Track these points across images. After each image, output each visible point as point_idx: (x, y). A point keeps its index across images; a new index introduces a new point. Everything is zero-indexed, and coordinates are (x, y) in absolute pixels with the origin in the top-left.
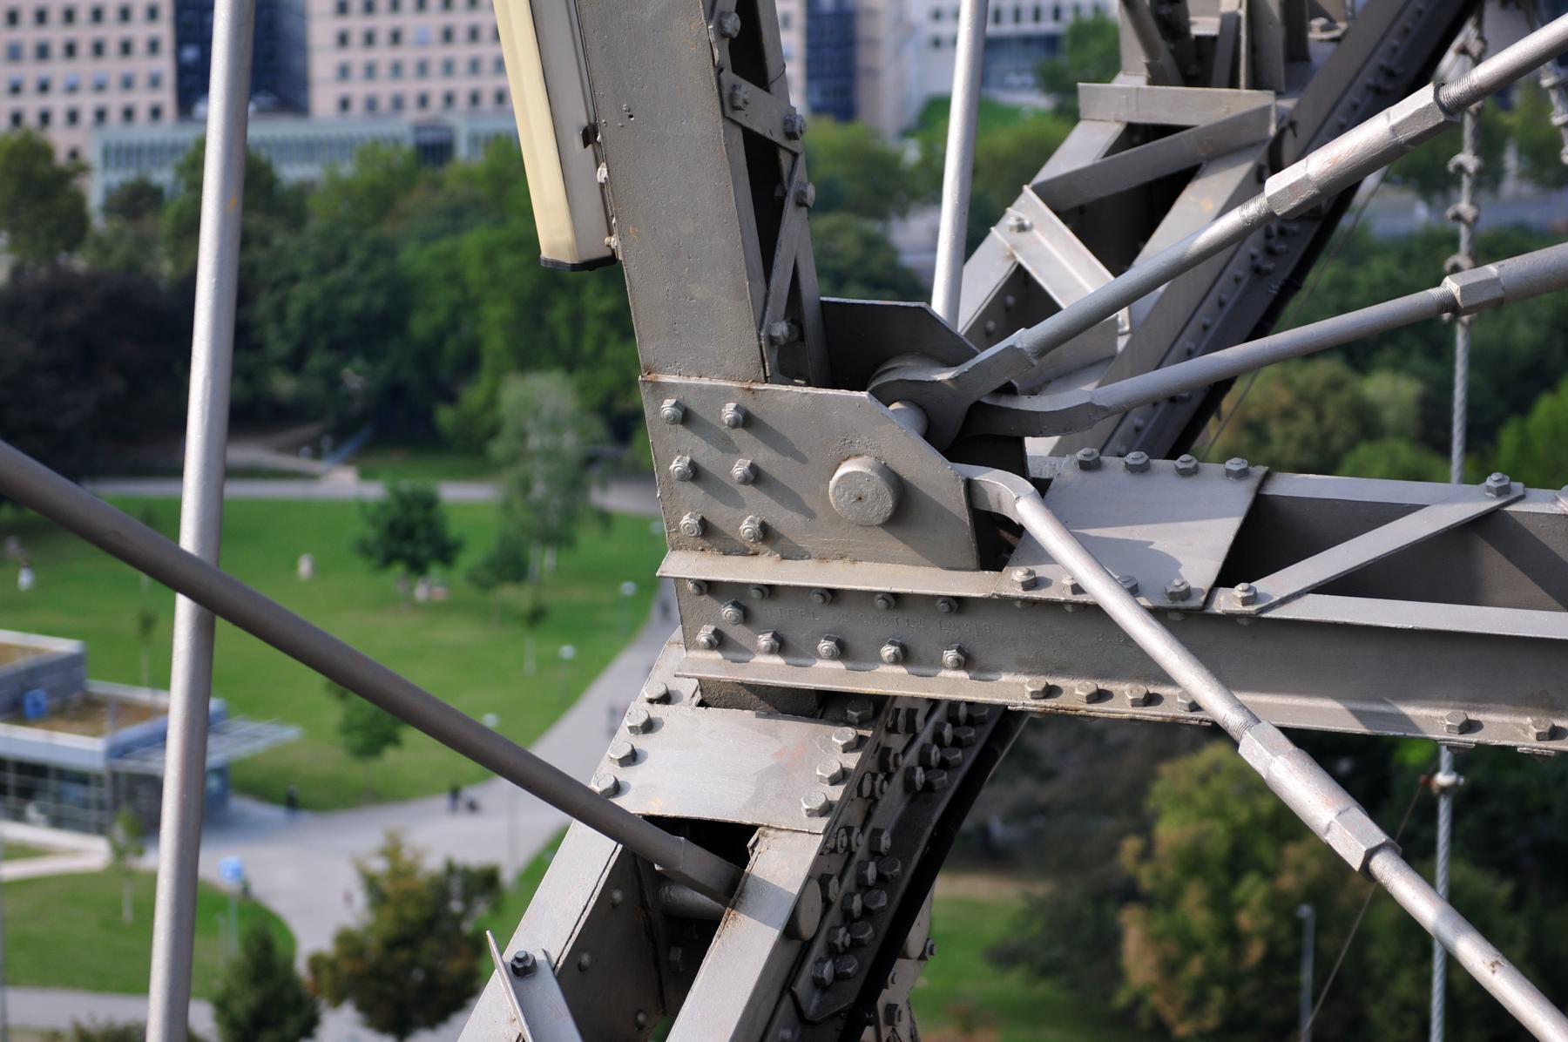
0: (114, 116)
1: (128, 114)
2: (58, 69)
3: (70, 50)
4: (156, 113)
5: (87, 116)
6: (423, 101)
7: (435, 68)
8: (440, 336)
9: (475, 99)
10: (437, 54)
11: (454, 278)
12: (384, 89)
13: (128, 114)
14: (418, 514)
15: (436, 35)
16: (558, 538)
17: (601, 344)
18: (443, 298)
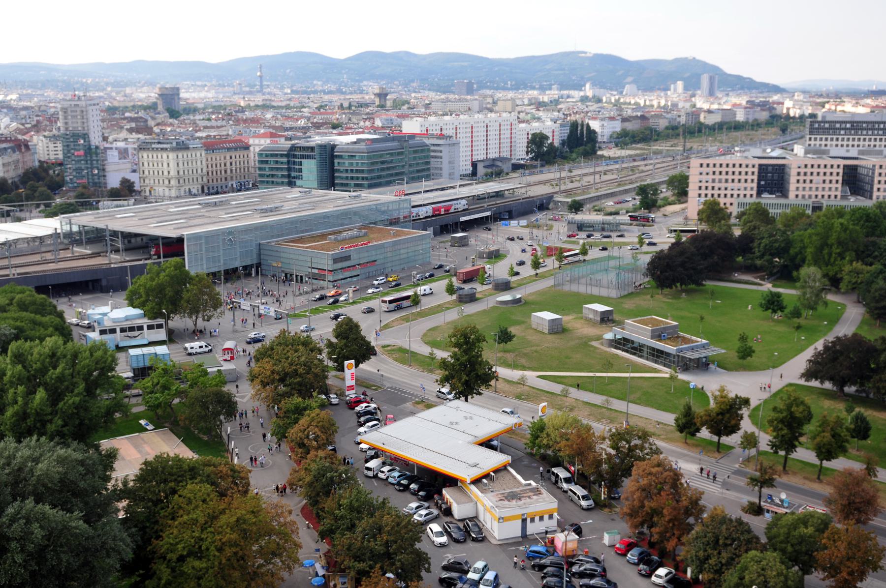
0: (742, 196)
1: (745, 196)
2: (730, 185)
3: (733, 181)
4: (751, 196)
5: (735, 196)
6: (816, 196)
7: (820, 189)
8: (797, 254)
9: (829, 196)
10: (821, 186)
11: (802, 241)
12: (807, 193)
13: (745, 196)
14: (776, 298)
15: (822, 181)
16: (813, 308)
17: (836, 260)
18: (798, 245)
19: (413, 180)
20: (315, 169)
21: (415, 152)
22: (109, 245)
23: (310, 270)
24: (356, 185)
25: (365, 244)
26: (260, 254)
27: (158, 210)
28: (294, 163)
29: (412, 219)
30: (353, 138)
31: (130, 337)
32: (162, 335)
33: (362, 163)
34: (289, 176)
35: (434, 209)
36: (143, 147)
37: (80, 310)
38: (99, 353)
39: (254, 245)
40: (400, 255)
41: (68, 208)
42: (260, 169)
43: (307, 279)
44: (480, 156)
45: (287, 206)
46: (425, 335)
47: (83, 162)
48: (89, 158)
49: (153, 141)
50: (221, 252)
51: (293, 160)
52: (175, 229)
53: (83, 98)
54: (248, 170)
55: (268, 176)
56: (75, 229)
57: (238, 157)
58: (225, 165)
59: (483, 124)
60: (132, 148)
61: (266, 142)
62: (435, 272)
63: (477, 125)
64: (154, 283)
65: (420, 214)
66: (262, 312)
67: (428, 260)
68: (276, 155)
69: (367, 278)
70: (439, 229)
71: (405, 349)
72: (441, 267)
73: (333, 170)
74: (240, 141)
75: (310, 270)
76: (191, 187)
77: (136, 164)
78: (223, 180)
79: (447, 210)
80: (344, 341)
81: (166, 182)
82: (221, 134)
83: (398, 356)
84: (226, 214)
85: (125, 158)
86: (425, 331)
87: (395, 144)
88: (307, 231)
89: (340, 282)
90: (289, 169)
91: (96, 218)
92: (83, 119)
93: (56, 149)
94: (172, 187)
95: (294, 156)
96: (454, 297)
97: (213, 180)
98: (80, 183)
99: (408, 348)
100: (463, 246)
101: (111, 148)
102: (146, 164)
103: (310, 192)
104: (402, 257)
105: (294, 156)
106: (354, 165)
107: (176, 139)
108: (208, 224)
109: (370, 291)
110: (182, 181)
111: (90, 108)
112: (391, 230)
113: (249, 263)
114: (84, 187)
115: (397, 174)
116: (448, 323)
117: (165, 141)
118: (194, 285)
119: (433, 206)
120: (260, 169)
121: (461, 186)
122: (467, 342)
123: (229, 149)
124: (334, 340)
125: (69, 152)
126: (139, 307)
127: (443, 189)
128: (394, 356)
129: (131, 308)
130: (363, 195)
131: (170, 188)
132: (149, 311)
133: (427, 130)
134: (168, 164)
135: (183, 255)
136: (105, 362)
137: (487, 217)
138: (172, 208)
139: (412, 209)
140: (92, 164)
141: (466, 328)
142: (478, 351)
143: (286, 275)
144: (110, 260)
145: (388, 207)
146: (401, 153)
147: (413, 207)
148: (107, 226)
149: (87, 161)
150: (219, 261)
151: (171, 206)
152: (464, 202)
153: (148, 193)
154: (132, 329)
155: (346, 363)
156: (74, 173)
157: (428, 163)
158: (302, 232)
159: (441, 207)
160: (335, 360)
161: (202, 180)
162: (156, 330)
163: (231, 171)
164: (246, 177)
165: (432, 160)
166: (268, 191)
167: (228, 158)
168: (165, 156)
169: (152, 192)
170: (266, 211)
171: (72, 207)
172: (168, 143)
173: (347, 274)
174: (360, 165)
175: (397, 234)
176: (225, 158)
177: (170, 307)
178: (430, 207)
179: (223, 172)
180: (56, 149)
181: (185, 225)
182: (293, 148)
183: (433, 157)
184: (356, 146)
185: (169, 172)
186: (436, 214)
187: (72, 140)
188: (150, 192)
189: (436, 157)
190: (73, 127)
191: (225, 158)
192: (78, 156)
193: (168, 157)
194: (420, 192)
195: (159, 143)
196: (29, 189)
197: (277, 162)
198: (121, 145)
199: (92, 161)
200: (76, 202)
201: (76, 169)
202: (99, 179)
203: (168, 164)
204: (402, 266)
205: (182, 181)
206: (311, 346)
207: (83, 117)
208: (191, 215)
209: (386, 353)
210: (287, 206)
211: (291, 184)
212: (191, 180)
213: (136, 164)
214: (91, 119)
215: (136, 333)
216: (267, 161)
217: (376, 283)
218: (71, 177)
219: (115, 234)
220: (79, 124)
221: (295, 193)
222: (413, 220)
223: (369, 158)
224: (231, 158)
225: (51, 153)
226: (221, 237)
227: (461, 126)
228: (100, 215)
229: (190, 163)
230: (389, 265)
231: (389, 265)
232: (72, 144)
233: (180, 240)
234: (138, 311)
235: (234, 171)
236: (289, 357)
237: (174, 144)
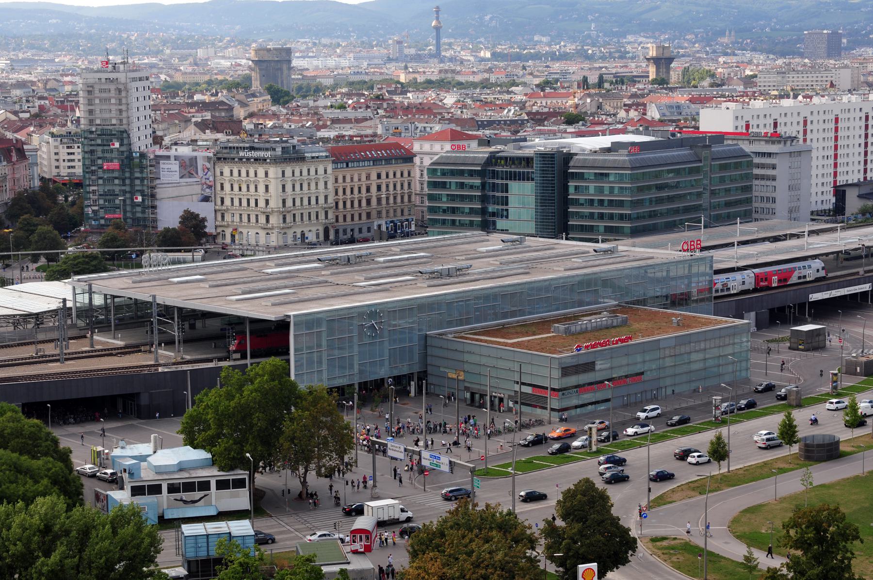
19: (717, 220)
20: (531, 201)
21: (724, 167)
22: (156, 332)
23: (517, 387)
24: (609, 230)
25: (622, 341)
26: (425, 356)
28: (494, 187)
29: (714, 294)
30: (605, 141)
31: (185, 502)
32: (241, 500)
33: (621, 188)
34: (483, 212)
35: (757, 276)
36: (223, 156)
37: (100, 448)
38: (128, 530)
39: (416, 339)
40: (690, 362)
41: (87, 263)
42: (431, 198)
43: (511, 404)
44: (851, 174)
45: (479, 266)
46: (735, 521)
47: (117, 182)
48: (127, 175)
49: (242, 145)
50: (356, 349)
51: (491, 181)
52: (274, 305)
53: (122, 67)
54: (410, 201)
55: (444, 211)
56: (98, 301)
57: (391, 175)
58: (368, 190)
59: (858, 114)
60: (204, 157)
61: (444, 148)
62: (757, 398)
63: (847, 115)
64: (232, 404)
65: (730, 285)
66: (425, 463)
67: (744, 374)
68: (461, 173)
69: (625, 406)
70: (767, 316)
71: (697, 547)
72: (769, 388)
73: (566, 201)
74: (397, 146)
75: (517, 387)
76: (306, 230)
77: (210, 187)
78: (364, 217)
79: (784, 278)
80: (578, 526)
81: (262, 219)
82: (363, 133)
83: (682, 559)
84: (367, 279)
85: (191, 175)
86: (735, 513)
87: (684, 152)
88: (513, 314)
89: (573, 412)
90: (484, 199)
91: (134, 282)
92: (120, 104)
93: (72, 157)
94: (272, 228)
95: (495, 174)
96: (795, 449)
97: (345, 217)
98: (110, 220)
99: (703, 546)
100: (816, 349)
101: (168, 157)
102: (227, 187)
103: (521, 242)
104: (694, 367)
105: (495, 174)
106: (607, 192)
107: (282, 141)
108: (333, 297)
109: (630, 431)
110: (289, 218)
111: (134, 85)
112: (676, 316)
113: (405, 371)
114: (118, 227)
115: (687, 210)
116: (783, 500)
117: (262, 146)
118: (304, 409)
119: (757, 271)
120: (431, 198)
121: (812, 233)
122: (820, 540)
123: (376, 161)
124: (560, 523)
125: (93, 163)
126: (203, 447)
127: (776, 239)
128: (674, 559)
129: (189, 447)
130: (620, 248)
131: (268, 231)
132: (221, 454)
133: (747, 127)
134: (267, 187)
135: (287, 353)
136: (138, 546)
137: (864, 294)
138: (270, 267)
139: (715, 277)
140: (132, 185)
141: (819, 511)
142: (844, 558)
143: (473, 395)
144: (157, 360)
145: (668, 271)
146: (697, 170)
147: (718, 272)
148: (154, 297)
149: (124, 180)
150: (351, 366)
151: (268, 263)
152: (818, 264)
153: (228, 240)
154: (189, 487)
155: (582, 567)
156: (101, 202)
157: (748, 189)
158: (505, 315)
159: (771, 274)
160: (561, 562)
161: (326, 217)
162: (231, 490)
163: (379, 200)
164: (406, 212)
165: (756, 182)
166: (444, 239)
167: (374, 176)
168: (261, 172)
169: (237, 237)
170: (439, 275)
171: (94, 263)
172: (267, 149)
173: (588, 397)
174: (616, 191)
175: (684, 324)
176: (368, 177)
177: (259, 448)
178: (749, 275)
180: (72, 157)
181: (292, 298)
182: (493, 159)
183: (757, 177)
184: (610, 157)
185: (267, 202)
186: (761, 285)
187: (99, 142)
188: (233, 236)
189: (763, 177)
190: (103, 120)
191: (368, 177)
192: (108, 170)
193: (266, 174)
194: (731, 245)
195: (252, 149)
196: (21, 229)
197: (462, 186)
198: (185, 151)
199: (132, 179)
200: (102, 253)
201: (105, 194)
202: (143, 212)
203: (267, 187)
204: (693, 386)
205: (289, 218)
206: (515, 533)
207: (120, 100)
208: (304, 281)
209: (660, 552)
210: (479, 266)
211: (487, 226)
212: (306, 218)
213: (210, 187)
214: (135, 105)
215: (197, 495)
216: (445, 183)
217: (642, 415)
218: (96, 208)
219: (167, 311)
220: (114, 114)
221: (494, 242)
222: (716, 298)
223: (633, 178)
224: (379, 176)
225: (62, 164)
226: (356, 322)
227: (815, 118)
228: (143, 277)
229: (305, 187)
230: (668, 382)
231: (668, 382)
232: (100, 149)
233: (283, 325)
234: (202, 455)
235: (384, 202)
236: (473, 551)
237: (279, 151)
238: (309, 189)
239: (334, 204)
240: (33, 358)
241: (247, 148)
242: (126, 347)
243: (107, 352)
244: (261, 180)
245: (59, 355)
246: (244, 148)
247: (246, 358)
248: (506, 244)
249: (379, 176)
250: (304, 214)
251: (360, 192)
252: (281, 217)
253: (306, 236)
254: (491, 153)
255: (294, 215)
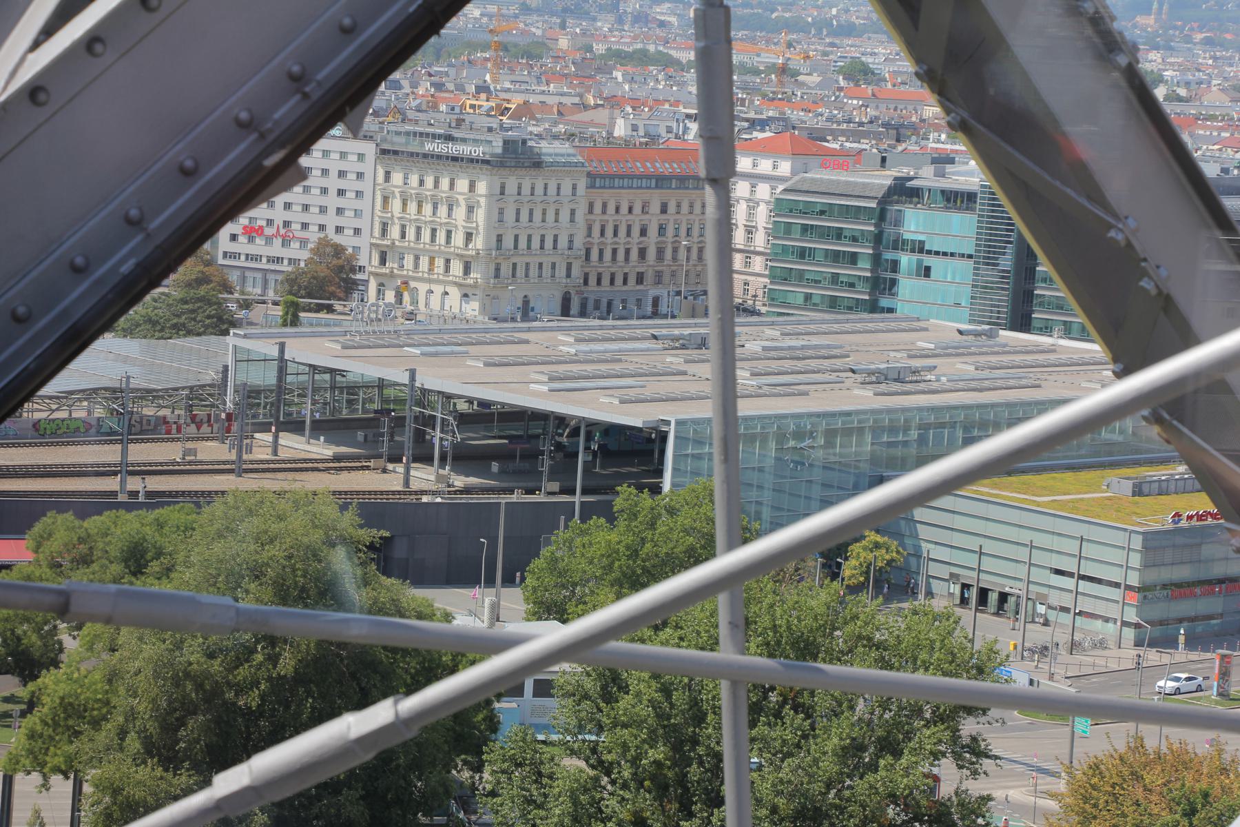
27: (527, 342)
58: (643, 232)
76: (530, 295)
91: (345, 347)
103: (991, 335)
143: (965, 587)
163: (660, 252)
167: (655, 208)
169: (406, 298)
179: (634, 255)
212: (534, 271)
224: (664, 210)
237: (498, 147)
238: (531, 221)
239: (583, 252)
240: (174, 463)
241: (440, 137)
242: (337, 458)
243: (310, 465)
244: (461, 198)
245: (233, 462)
246: (434, 136)
247: (572, 492)
248: (964, 337)
249: (664, 210)
250: (518, 267)
251: (629, 234)
252: (493, 267)
253: (531, 305)
254: (896, 179)
255: (515, 265)
